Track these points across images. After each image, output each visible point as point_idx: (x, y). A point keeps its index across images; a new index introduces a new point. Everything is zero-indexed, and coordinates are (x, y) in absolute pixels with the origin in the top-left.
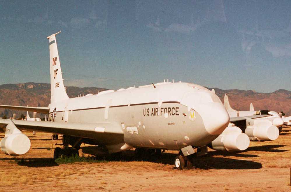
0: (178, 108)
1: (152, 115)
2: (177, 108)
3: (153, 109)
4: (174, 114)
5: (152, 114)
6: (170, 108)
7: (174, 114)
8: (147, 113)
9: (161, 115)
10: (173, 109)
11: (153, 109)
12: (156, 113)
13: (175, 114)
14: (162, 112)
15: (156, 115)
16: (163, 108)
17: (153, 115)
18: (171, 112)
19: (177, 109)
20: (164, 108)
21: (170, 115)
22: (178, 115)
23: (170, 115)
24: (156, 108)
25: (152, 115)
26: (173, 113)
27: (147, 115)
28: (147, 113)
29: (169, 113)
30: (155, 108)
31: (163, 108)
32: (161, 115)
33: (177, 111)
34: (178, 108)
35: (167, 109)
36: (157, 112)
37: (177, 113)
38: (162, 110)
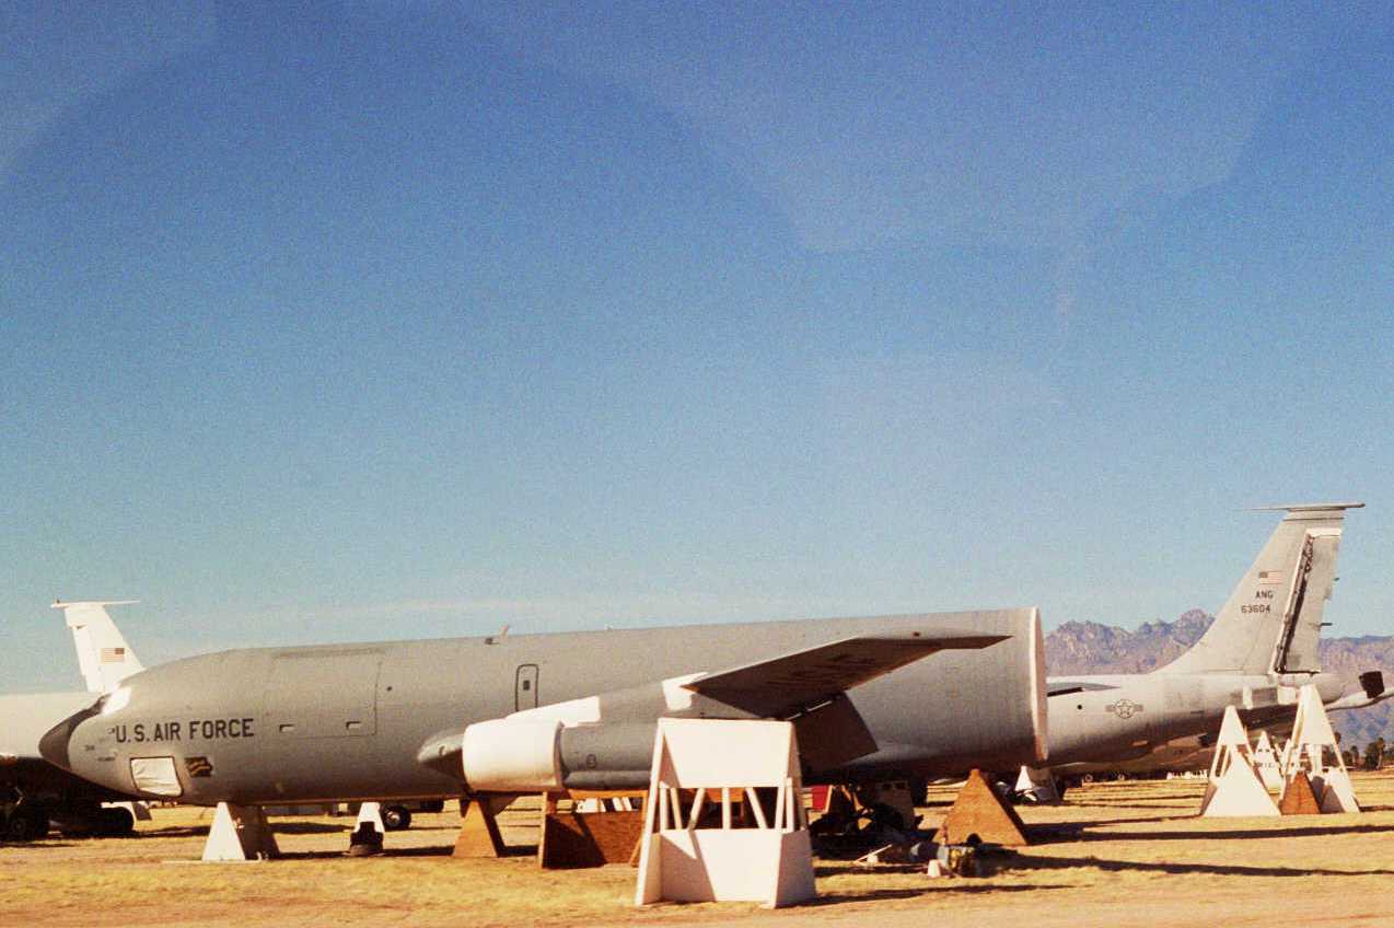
2: (245, 721)
10: (234, 724)
14: (193, 731)
16: (197, 723)
18: (227, 730)
19: (247, 724)
29: (220, 732)
31: (197, 723)
33: (245, 728)
34: (251, 720)
36: (177, 731)
37: (248, 731)
38: (194, 726)
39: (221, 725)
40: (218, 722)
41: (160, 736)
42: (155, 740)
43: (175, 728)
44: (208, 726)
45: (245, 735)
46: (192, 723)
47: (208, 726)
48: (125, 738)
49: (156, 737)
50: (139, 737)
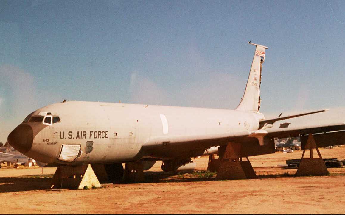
0: (108, 132)
1: (78, 138)
2: (106, 132)
4: (104, 137)
5: (78, 137)
6: (100, 132)
7: (104, 137)
8: (67, 135)
10: (103, 133)
13: (105, 137)
14: (91, 135)
15: (83, 138)
16: (93, 132)
17: (79, 138)
19: (107, 133)
20: (94, 132)
21: (100, 138)
22: (107, 137)
23: (100, 138)
24: (83, 132)
25: (77, 138)
26: (103, 136)
27: (67, 138)
28: (67, 135)
29: (99, 136)
30: (81, 132)
31: (93, 132)
32: (90, 138)
33: (106, 134)
34: (108, 132)
36: (85, 135)
37: (107, 136)
38: (91, 133)
40: (99, 132)
41: (79, 137)
42: (77, 138)
43: (85, 133)
44: (96, 133)
45: (106, 137)
46: (91, 132)
47: (96, 133)
48: (64, 137)
49: (77, 137)
50: (70, 137)
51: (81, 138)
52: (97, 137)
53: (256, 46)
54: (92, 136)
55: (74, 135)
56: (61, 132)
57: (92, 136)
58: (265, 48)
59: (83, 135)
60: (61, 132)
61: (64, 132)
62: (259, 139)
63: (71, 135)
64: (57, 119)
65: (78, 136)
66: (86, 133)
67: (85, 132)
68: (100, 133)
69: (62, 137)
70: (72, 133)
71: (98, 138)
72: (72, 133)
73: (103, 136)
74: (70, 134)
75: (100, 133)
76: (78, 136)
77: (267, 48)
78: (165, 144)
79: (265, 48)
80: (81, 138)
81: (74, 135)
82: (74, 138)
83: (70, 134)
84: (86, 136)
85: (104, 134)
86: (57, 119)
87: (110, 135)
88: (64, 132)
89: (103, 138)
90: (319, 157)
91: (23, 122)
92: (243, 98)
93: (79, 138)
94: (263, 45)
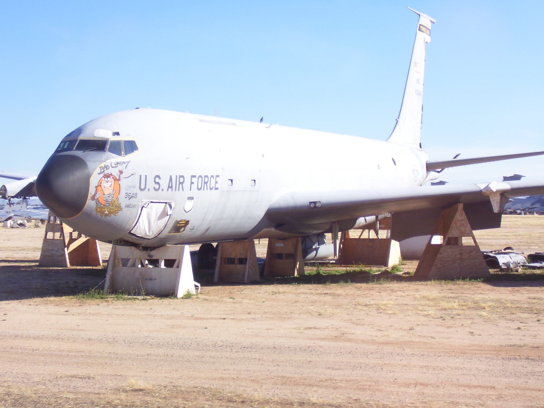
0: (218, 176)
1: (170, 189)
3: (171, 176)
5: (170, 187)
9: (190, 190)
10: (212, 178)
11: (171, 176)
12: (181, 185)
13: (214, 188)
14: (192, 183)
15: (179, 190)
16: (195, 176)
17: (172, 190)
18: (208, 184)
20: (197, 177)
22: (217, 189)
23: (207, 189)
24: (181, 176)
25: (168, 190)
26: (211, 187)
27: (152, 190)
28: (151, 184)
29: (205, 185)
30: (176, 176)
31: (195, 176)
33: (216, 182)
34: (218, 176)
35: (202, 178)
36: (182, 183)
39: (206, 180)
40: (206, 176)
41: (171, 187)
42: (168, 190)
44: (200, 179)
45: (217, 189)
47: (200, 179)
48: (145, 188)
49: (169, 187)
50: (157, 186)
51: (176, 190)
52: (201, 188)
53: (419, 15)
54: (194, 186)
55: (164, 183)
56: (140, 176)
57: (194, 186)
58: (432, 22)
59: (180, 183)
60: (140, 176)
61: (146, 176)
62: (492, 199)
63: (158, 183)
64: (131, 146)
65: (170, 185)
66: (184, 178)
67: (182, 177)
68: (206, 179)
69: (143, 187)
70: (160, 178)
71: (204, 190)
72: (160, 178)
73: (211, 187)
74: (157, 180)
75: (206, 179)
76: (170, 185)
77: (434, 21)
78: (312, 205)
79: (432, 22)
80: (176, 190)
81: (164, 183)
82: (163, 190)
83: (157, 180)
84: (184, 185)
85: (213, 181)
86: (131, 146)
87: (223, 183)
88: (146, 176)
89: (211, 189)
90: (377, 238)
91: (57, 151)
92: (398, 118)
93: (172, 190)
94: (429, 15)
